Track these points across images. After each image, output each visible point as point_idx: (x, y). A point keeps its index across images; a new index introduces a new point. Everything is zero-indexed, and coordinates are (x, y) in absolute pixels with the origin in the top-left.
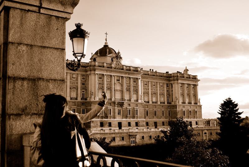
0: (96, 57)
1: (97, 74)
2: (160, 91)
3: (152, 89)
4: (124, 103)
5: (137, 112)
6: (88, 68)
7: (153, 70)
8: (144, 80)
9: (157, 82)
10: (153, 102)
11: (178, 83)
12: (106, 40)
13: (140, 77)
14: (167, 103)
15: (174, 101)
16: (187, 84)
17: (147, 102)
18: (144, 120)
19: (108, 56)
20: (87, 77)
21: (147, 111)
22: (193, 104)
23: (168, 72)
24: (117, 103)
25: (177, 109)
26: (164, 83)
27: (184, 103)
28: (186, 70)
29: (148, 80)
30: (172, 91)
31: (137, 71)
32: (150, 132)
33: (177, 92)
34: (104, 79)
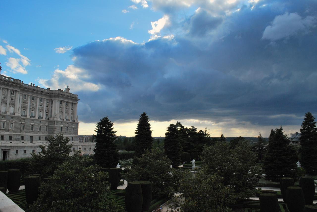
7: (34, 85)
14: (46, 118)
17: (24, 116)
18: (20, 134)
21: (24, 125)
23: (50, 89)
25: (55, 125)
29: (28, 94)
30: (52, 107)
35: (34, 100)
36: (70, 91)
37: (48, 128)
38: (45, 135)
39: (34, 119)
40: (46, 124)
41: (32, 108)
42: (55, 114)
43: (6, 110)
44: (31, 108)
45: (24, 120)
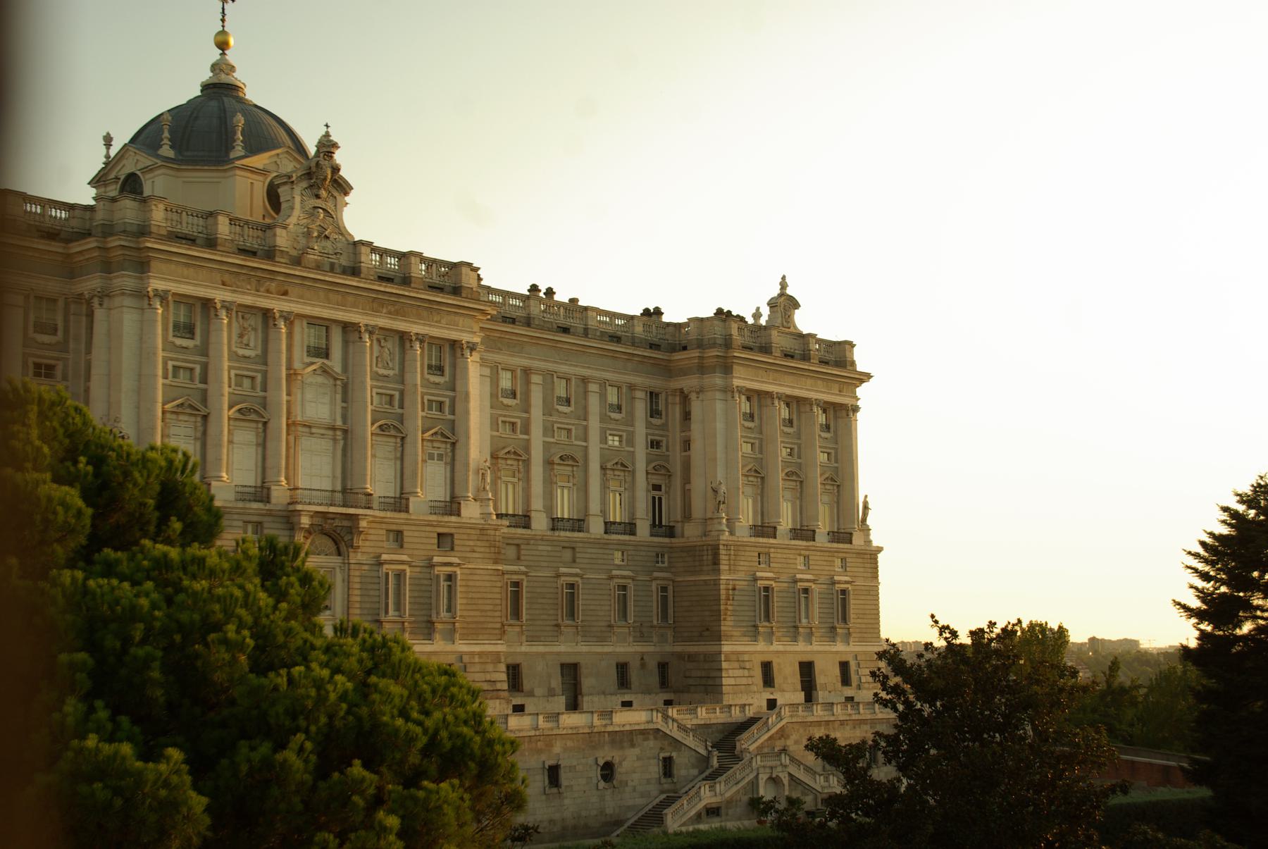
0: (148, 170)
1: (163, 296)
2: (604, 440)
3: (548, 430)
4: (363, 524)
5: (449, 586)
6: (91, 243)
7: (550, 292)
8: (497, 357)
9: (585, 381)
10: (554, 520)
11: (728, 390)
12: (223, 45)
13: (477, 340)
14: (653, 525)
15: (697, 510)
16: (790, 401)
19: (246, 168)
20: (72, 318)
22: (822, 539)
23: (658, 312)
24: (305, 521)
25: (718, 571)
26: (632, 387)
27: (764, 529)
28: (784, 304)
29: (526, 362)
30: (687, 445)
31: (456, 291)
32: (549, 739)
33: (720, 455)
34: (213, 339)
35: (568, 401)
36: (804, 321)
37: (670, 599)
38: (658, 649)
39: (581, 535)
40: (661, 569)
41: (561, 458)
42: (715, 491)
43: (402, 488)
44: (557, 460)
45: (518, 545)
